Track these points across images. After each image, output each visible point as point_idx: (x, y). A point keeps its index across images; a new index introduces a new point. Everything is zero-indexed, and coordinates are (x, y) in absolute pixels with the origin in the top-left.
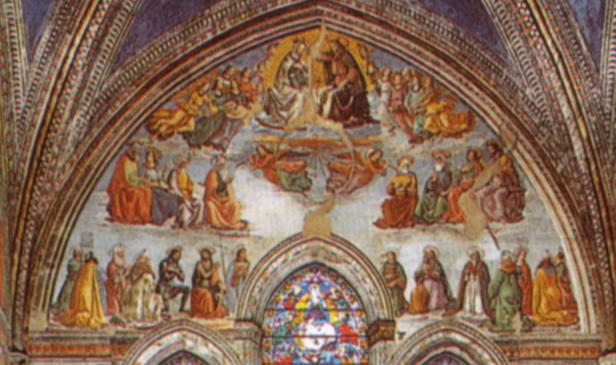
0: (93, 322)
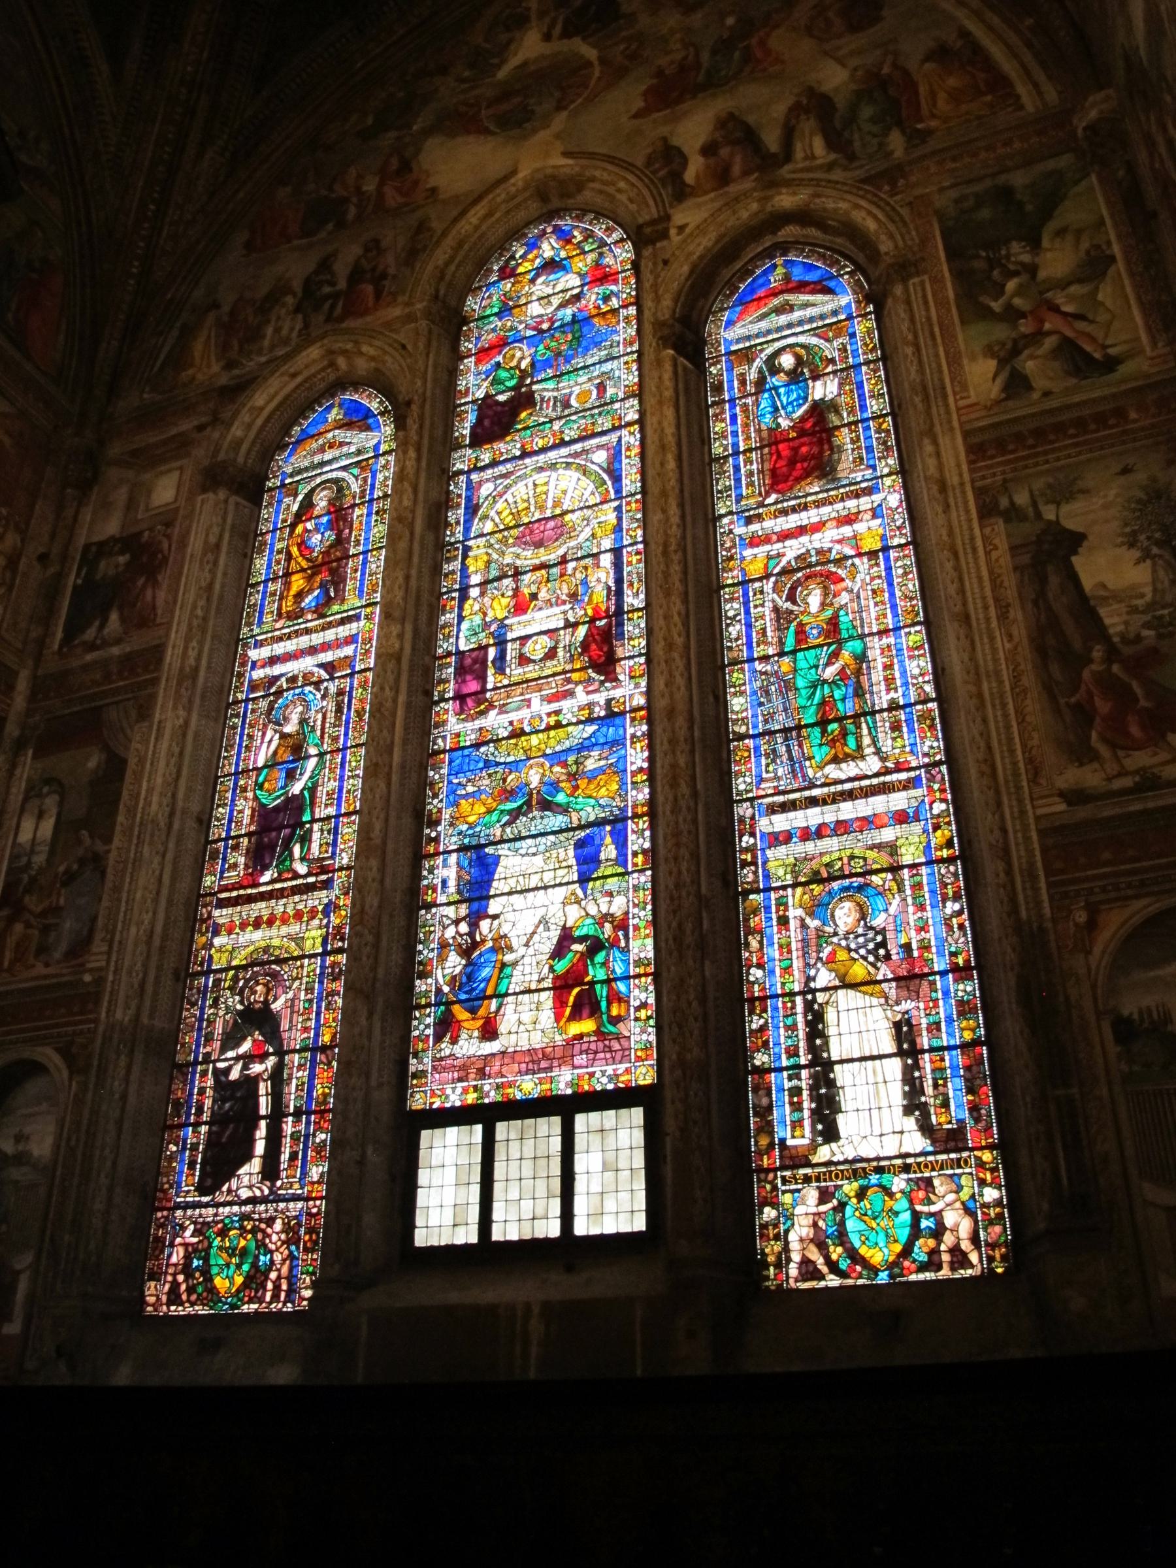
0: (200, 377)
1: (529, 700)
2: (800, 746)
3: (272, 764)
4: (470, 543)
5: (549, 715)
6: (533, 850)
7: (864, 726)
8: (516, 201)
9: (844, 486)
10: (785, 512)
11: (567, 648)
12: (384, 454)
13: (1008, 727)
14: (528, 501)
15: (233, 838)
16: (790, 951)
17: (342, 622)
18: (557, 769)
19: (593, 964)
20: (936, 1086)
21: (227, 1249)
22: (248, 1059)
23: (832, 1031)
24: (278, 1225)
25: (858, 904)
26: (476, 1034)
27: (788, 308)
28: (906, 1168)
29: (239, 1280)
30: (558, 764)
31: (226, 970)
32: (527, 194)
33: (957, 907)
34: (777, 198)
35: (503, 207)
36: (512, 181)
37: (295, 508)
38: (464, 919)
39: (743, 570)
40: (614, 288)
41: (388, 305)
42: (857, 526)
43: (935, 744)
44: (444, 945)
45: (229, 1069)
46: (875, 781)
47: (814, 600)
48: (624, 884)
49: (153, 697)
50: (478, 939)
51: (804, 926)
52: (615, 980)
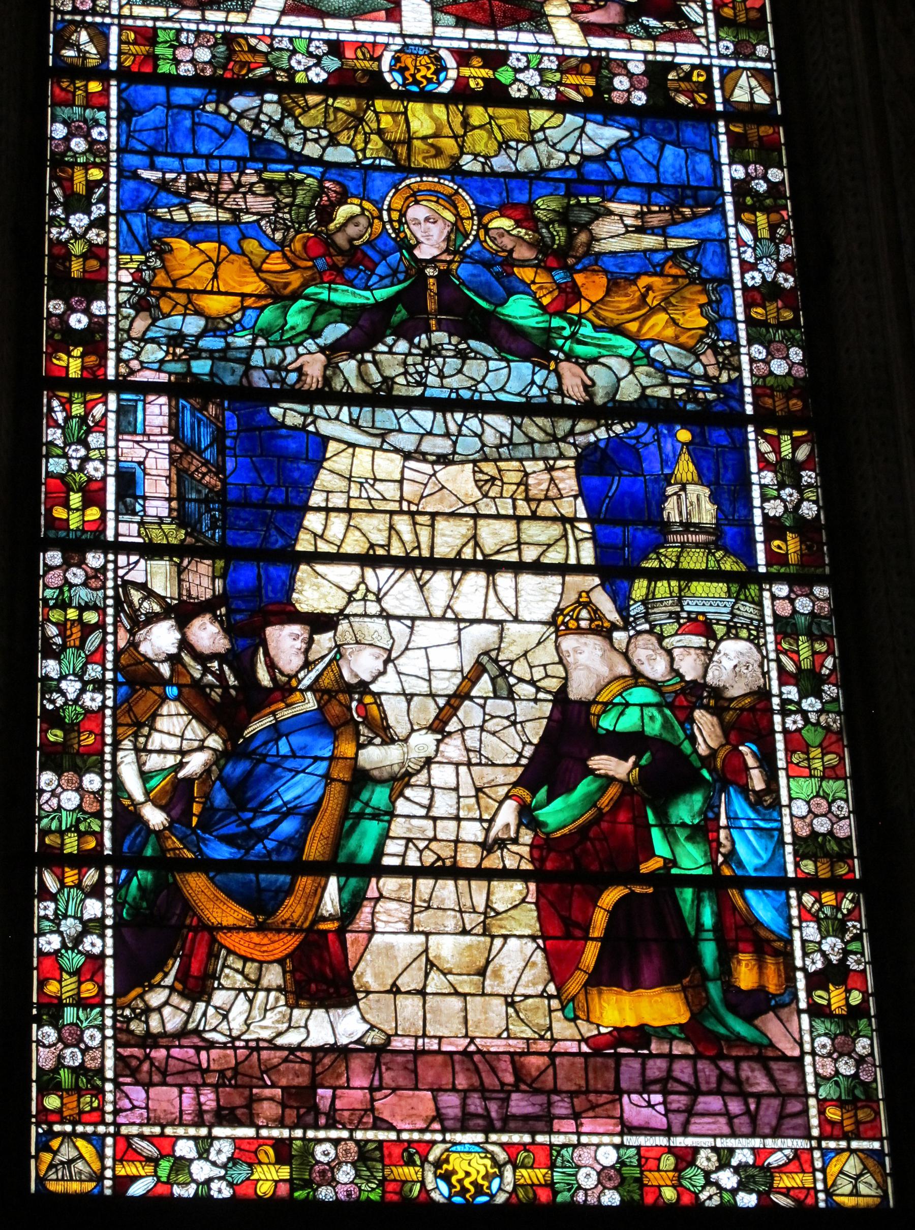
5: (463, 57)
6: (443, 446)
26: (273, 976)
30: (504, 210)
38: (206, 607)
48: (747, 610)
52: (745, 883)
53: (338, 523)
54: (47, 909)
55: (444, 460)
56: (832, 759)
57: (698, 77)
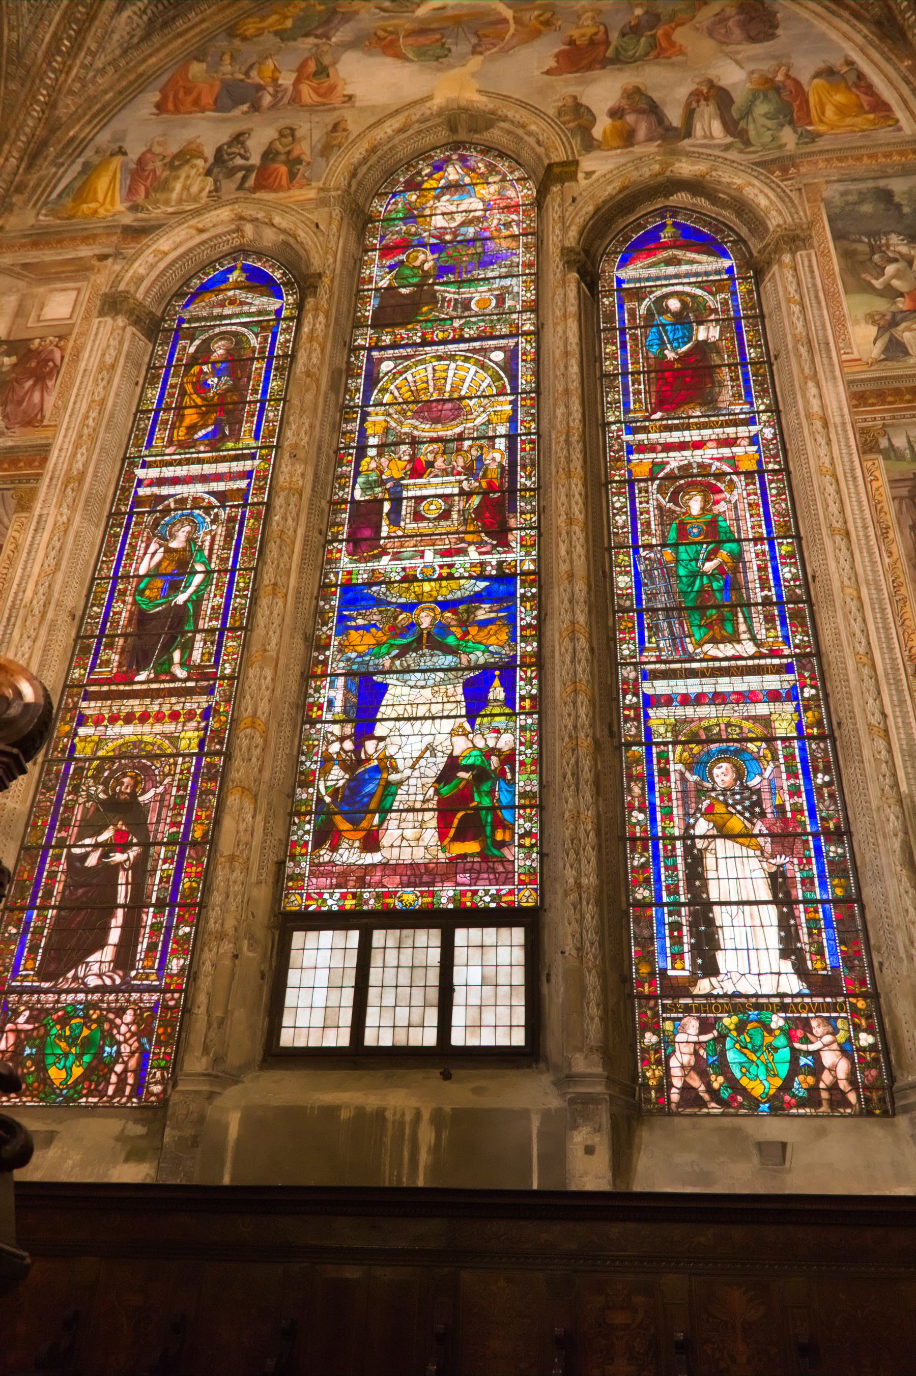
0: (102, 211)
1: (423, 552)
2: (681, 624)
3: (153, 574)
4: (370, 409)
5: (441, 567)
6: (423, 683)
7: (740, 615)
8: (429, 124)
9: (724, 415)
10: (670, 429)
11: (461, 512)
12: (285, 319)
13: (887, 629)
14: (427, 382)
15: (107, 636)
16: (670, 800)
17: (237, 458)
18: (449, 615)
19: (479, 793)
20: (810, 934)
21: (66, 1039)
22: (108, 848)
23: (711, 874)
24: (128, 1017)
25: (735, 766)
26: (357, 844)
27: (678, 262)
28: (784, 1008)
29: (77, 1071)
31: (91, 760)
32: (438, 120)
33: (827, 778)
34: (677, 165)
35: (416, 127)
36: (428, 104)
37: (192, 350)
38: (349, 737)
39: (630, 472)
40: (514, 217)
41: (301, 187)
42: (735, 449)
43: (806, 639)
44: (327, 760)
45: (86, 856)
46: (750, 663)
47: (696, 505)
48: (511, 724)
49: (33, 492)
50: (363, 756)
51: (683, 779)
52: (501, 808)
53: (390, 708)
54: (295, 828)
55: (423, 687)
56: (533, 768)
57: (513, 564)
